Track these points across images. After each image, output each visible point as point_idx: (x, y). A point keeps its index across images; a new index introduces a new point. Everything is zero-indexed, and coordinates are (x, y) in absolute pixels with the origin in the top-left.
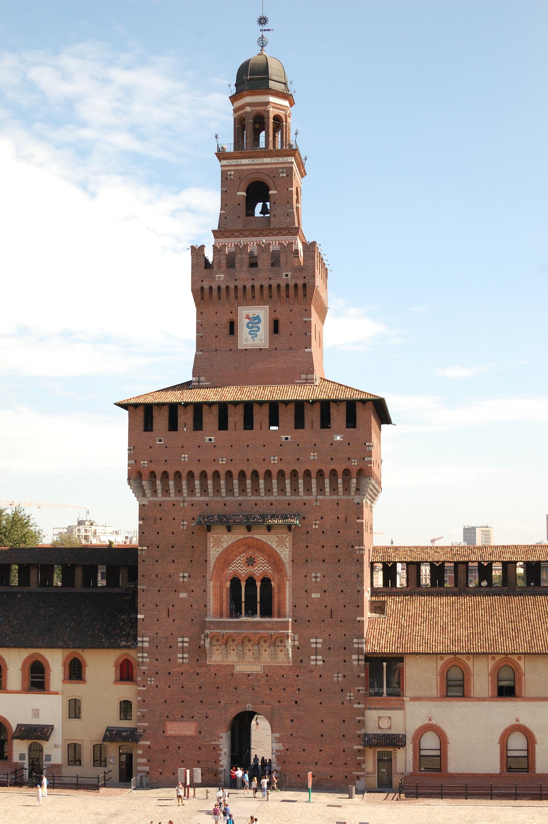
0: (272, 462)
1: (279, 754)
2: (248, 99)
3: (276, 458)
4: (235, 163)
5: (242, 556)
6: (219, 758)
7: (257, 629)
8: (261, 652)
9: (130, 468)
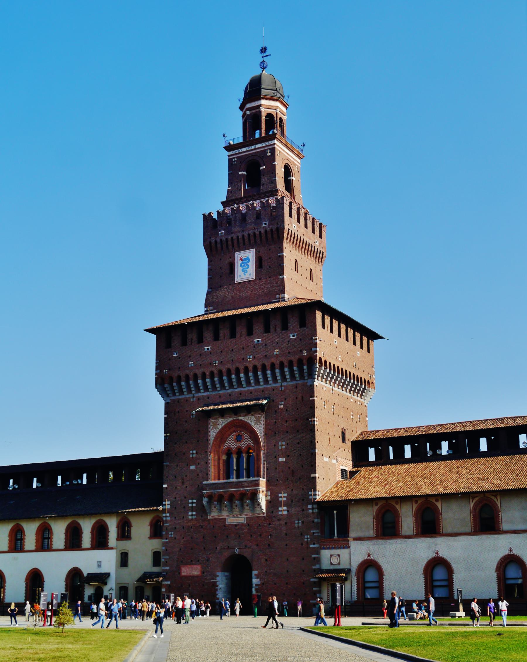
0: (249, 360)
1: (257, 587)
2: (248, 106)
3: (251, 357)
4: (237, 152)
5: (233, 434)
6: (216, 592)
9: (157, 376)
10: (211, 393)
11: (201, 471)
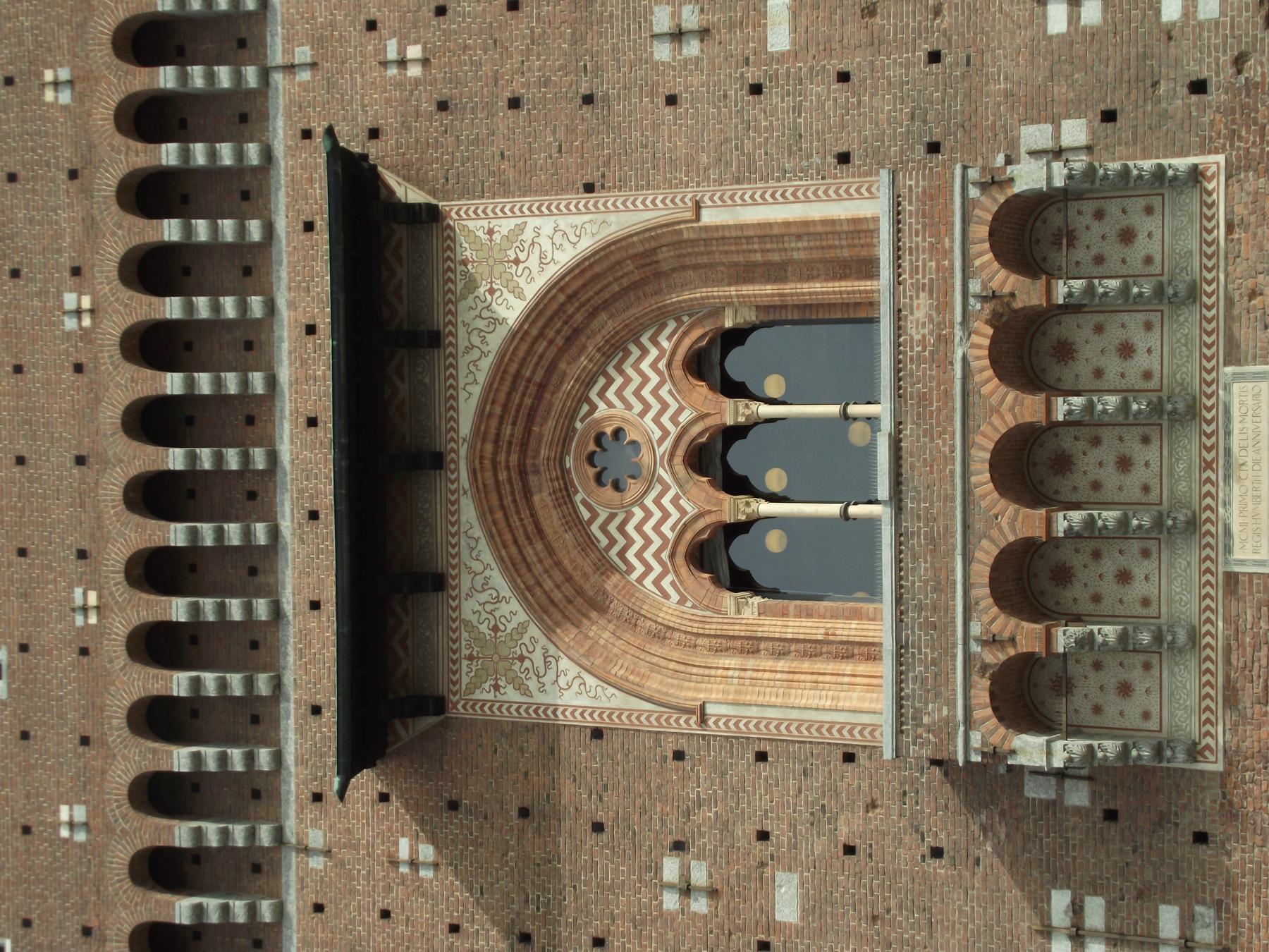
0: (87, 322)
7: (948, 394)
11: (821, 816)
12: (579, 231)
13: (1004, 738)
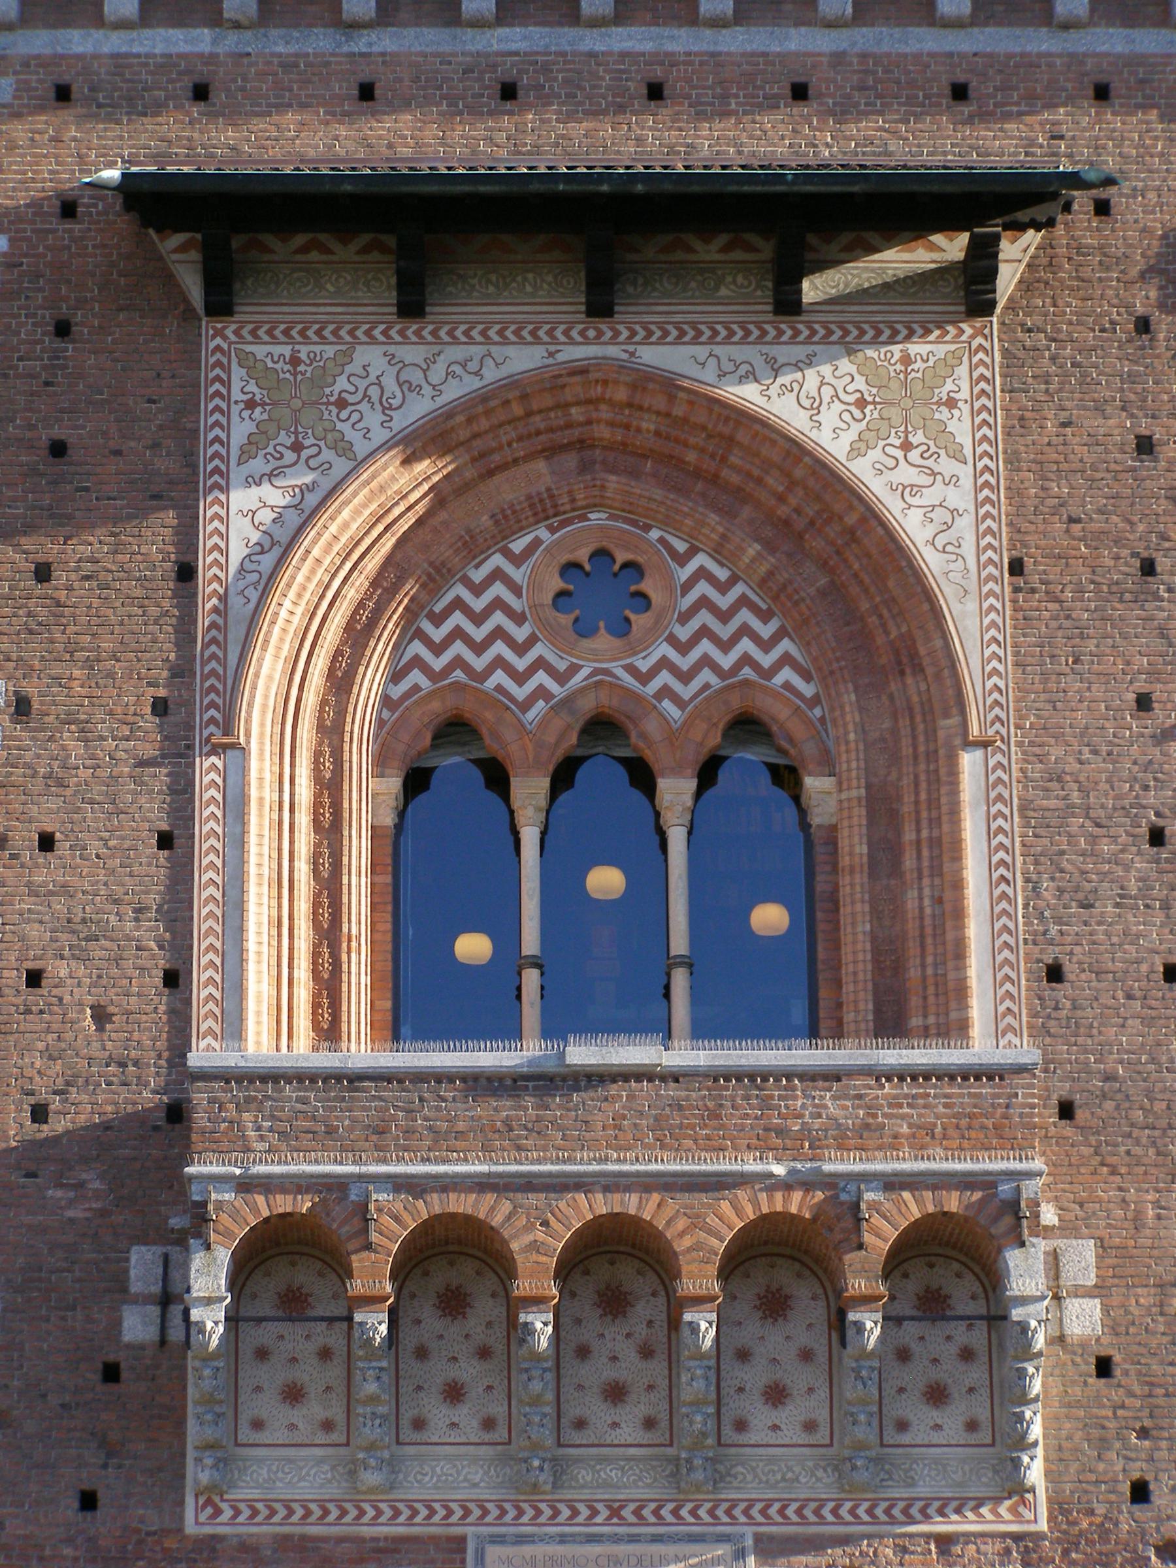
5: (518, 546)
8: (734, 1406)
10: (231, 41)
12: (950, 550)
13: (229, 1234)
